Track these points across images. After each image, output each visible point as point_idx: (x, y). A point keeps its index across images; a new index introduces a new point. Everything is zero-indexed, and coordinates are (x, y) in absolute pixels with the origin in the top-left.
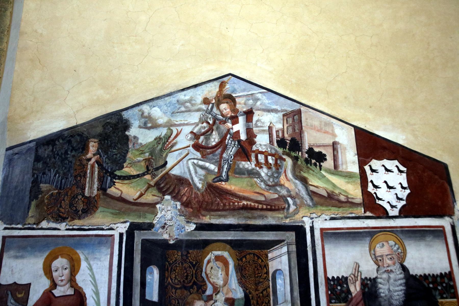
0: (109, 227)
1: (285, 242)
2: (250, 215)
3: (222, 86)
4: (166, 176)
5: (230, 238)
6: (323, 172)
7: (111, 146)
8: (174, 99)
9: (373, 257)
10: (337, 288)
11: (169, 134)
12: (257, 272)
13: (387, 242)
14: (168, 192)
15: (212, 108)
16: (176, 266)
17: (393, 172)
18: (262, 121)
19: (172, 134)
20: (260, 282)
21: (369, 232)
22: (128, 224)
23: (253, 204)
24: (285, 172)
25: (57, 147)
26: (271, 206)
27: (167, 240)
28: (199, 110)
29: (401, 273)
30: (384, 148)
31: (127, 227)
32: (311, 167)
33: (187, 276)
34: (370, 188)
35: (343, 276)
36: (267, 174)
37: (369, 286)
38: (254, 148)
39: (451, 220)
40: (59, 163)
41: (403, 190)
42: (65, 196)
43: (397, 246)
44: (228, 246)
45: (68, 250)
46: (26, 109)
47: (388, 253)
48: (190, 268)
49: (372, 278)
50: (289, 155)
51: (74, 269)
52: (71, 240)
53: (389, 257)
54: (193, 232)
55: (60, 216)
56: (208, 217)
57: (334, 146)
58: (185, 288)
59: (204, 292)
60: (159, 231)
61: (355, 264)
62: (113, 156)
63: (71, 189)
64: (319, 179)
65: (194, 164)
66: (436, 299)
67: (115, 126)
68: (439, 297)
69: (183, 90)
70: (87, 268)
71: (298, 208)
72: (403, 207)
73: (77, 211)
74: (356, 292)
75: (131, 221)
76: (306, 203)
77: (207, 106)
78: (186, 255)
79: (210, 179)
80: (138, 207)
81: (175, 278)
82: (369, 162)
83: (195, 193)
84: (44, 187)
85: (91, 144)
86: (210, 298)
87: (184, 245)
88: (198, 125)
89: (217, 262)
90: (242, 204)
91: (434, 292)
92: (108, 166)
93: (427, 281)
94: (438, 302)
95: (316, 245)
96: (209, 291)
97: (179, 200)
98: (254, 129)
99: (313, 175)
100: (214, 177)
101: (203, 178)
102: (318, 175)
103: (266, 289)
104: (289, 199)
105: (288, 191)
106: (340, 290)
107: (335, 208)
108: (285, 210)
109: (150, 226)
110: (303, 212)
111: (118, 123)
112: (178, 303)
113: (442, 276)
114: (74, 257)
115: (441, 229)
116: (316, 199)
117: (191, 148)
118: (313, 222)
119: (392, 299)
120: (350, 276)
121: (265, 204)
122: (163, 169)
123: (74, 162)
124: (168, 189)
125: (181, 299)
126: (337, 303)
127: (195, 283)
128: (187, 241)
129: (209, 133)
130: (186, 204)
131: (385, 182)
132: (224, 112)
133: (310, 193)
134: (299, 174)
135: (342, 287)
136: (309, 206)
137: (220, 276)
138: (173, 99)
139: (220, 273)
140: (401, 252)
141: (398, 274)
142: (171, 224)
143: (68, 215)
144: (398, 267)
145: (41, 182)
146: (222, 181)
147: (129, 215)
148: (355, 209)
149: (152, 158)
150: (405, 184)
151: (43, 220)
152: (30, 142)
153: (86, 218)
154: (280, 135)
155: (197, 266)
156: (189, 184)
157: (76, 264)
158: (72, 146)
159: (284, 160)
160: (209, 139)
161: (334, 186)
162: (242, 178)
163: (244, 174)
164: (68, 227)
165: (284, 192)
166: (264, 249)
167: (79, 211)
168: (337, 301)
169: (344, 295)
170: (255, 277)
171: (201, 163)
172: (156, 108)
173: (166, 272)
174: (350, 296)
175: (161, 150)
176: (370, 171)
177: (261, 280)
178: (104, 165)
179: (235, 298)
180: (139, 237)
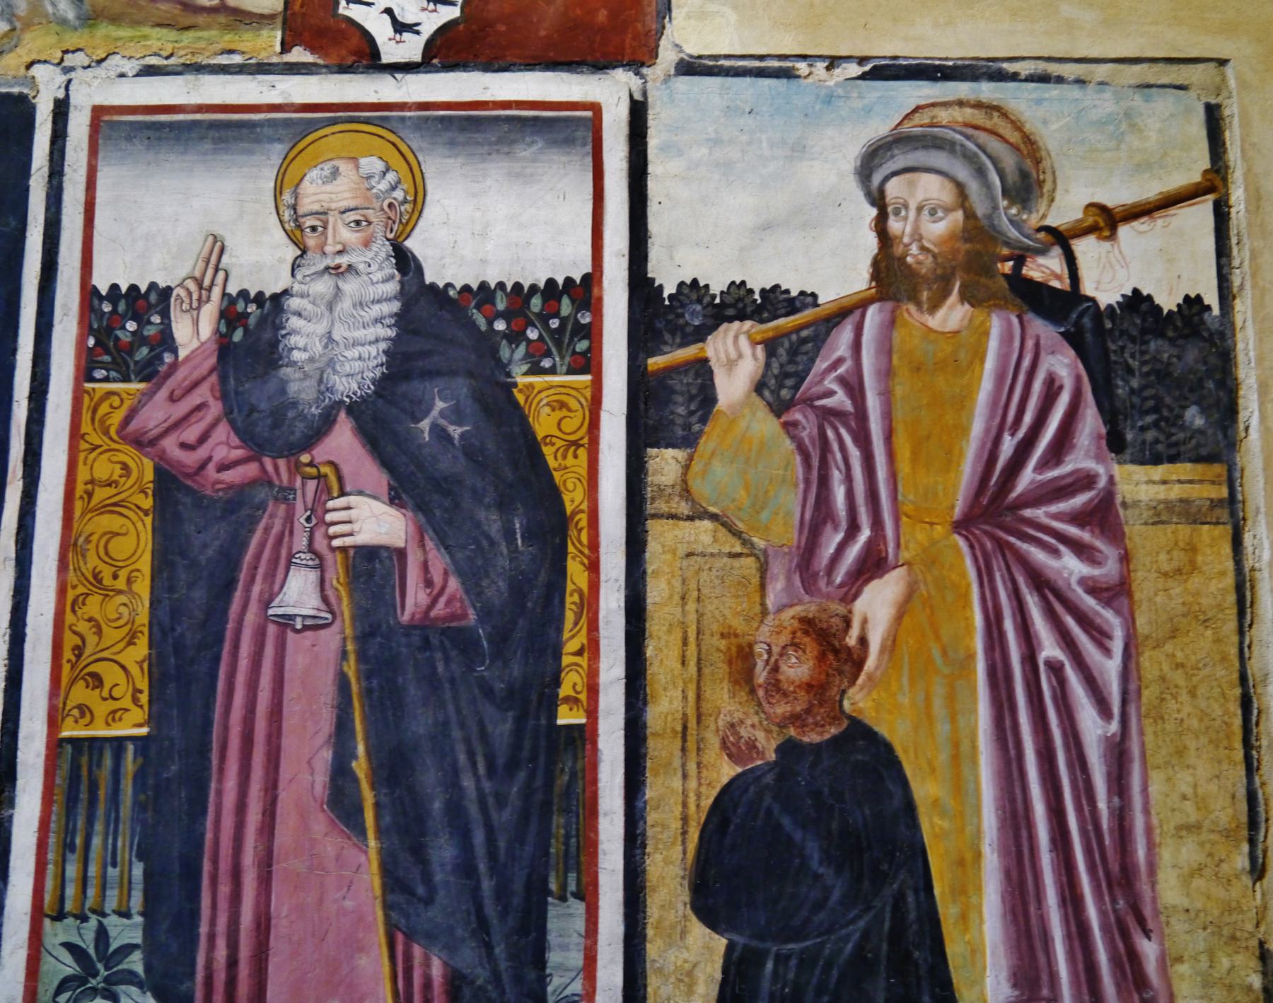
9: (287, 215)
10: (123, 328)
13: (354, 159)
21: (287, 123)
35: (153, 286)
37: (252, 321)
43: (391, 177)
47: (352, 204)
49: (268, 294)
53: (352, 216)
61: (211, 239)
66: (509, 375)
68: (525, 368)
74: (195, 344)
76: (50, 9)
91: (505, 353)
93: (488, 306)
94: (515, 385)
95: (66, 169)
106: (133, 333)
107: (165, 31)
113: (551, 289)
115: (589, 114)
118: (70, 81)
119: (335, 372)
126: (115, 381)
136: (63, 22)
140: (405, 201)
141: (377, 284)
144: (383, 255)
148: (248, 36)
168: (113, 374)
169: (145, 351)
174: (168, 358)
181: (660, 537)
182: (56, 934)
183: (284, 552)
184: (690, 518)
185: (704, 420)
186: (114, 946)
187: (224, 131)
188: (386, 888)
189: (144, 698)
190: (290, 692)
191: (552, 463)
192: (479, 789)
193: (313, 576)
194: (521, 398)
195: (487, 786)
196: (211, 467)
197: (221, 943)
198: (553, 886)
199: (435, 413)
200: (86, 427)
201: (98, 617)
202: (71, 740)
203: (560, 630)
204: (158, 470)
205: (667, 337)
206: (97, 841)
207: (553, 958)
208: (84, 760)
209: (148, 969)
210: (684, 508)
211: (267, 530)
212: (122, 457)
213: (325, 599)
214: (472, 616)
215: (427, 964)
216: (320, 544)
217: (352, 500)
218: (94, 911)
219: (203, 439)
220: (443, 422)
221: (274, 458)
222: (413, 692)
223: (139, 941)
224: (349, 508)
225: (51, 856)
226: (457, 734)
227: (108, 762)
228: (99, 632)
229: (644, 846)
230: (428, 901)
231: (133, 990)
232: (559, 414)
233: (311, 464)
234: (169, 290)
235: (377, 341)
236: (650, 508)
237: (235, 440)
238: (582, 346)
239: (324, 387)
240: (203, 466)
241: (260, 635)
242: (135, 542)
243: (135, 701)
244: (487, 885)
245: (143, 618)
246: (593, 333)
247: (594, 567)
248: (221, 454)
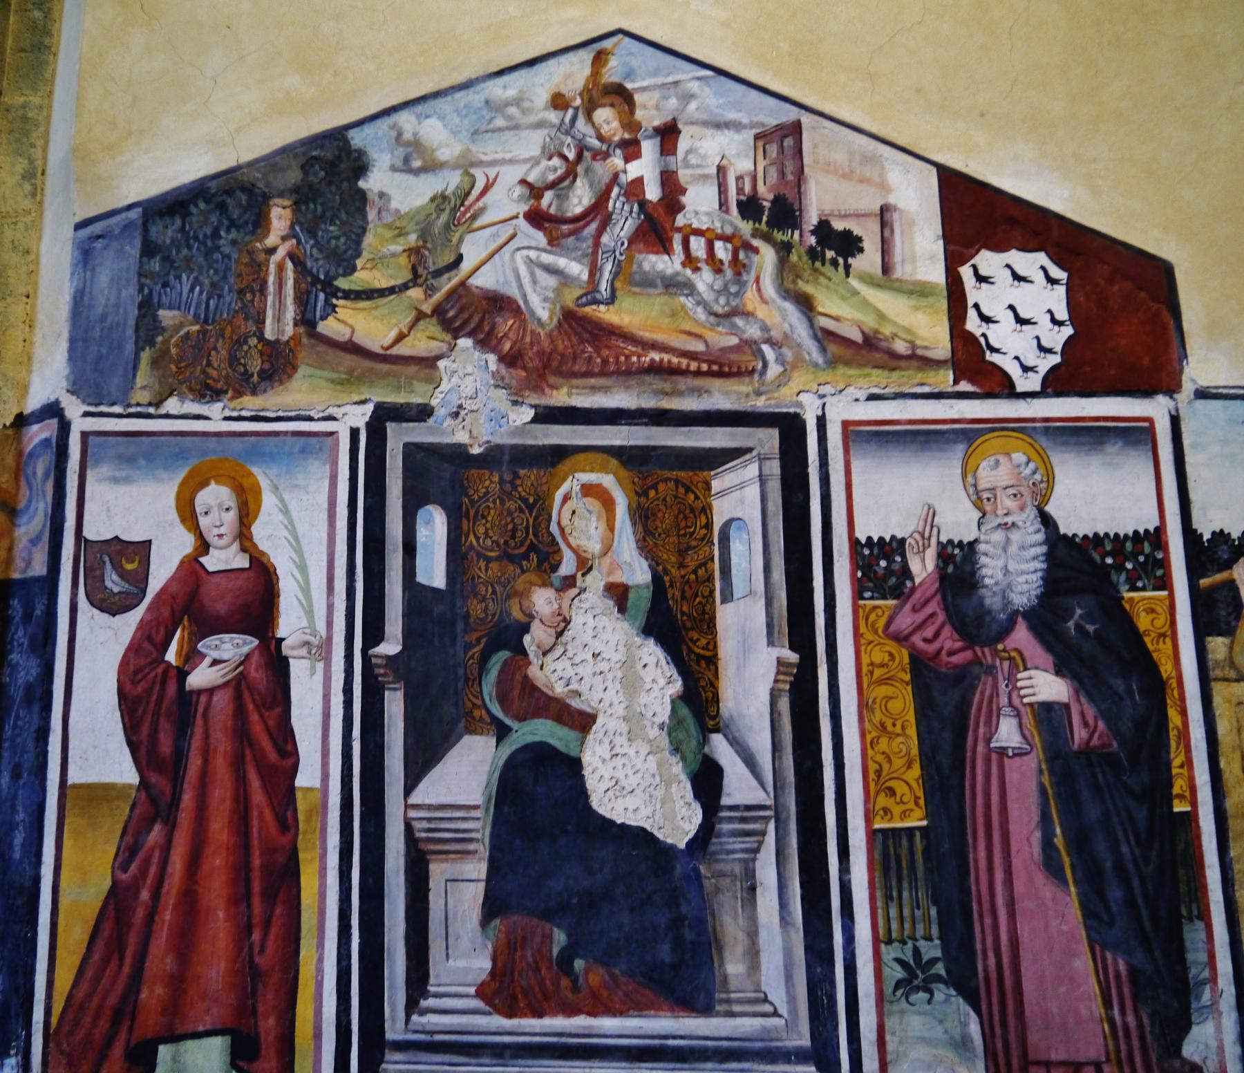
0: (326, 414)
1: (755, 453)
2: (667, 386)
3: (600, 59)
4: (461, 291)
5: (617, 443)
6: (853, 282)
7: (323, 216)
8: (477, 97)
9: (971, 490)
10: (878, 564)
11: (467, 188)
12: (683, 524)
13: (1008, 454)
14: (467, 330)
15: (574, 120)
16: (488, 507)
17: (1031, 282)
18: (702, 151)
19: (472, 187)
20: (689, 548)
21: (963, 431)
22: (369, 408)
23: (675, 360)
24: (757, 281)
25: (194, 219)
26: (721, 365)
27: (465, 445)
28: (540, 125)
29: (1038, 531)
30: (1013, 222)
31: (369, 414)
32: (823, 269)
33: (514, 530)
34: (973, 324)
35: (893, 537)
36: (711, 287)
37: (958, 559)
38: (680, 220)
39: (1171, 404)
40: (201, 259)
41: (1056, 328)
42: (217, 341)
43: (1032, 465)
44: (614, 462)
45: (228, 467)
46: (114, 125)
47: (1010, 483)
48: (521, 511)
50: (767, 238)
51: (247, 512)
52: (236, 444)
53: (1011, 491)
54: (528, 426)
55: (208, 387)
56: (565, 390)
57: (885, 215)
58: (511, 558)
59: (555, 568)
60: (445, 424)
62: (329, 242)
63: (230, 322)
64: (844, 299)
65: (530, 262)
66: (1118, 592)
67: (332, 167)
68: (1127, 587)
69: (500, 73)
70: (277, 510)
71: (789, 369)
72: (1054, 369)
73: (247, 376)
74: (924, 575)
75: (376, 399)
77: (561, 113)
78: (512, 482)
79: (570, 297)
80: (395, 368)
81: (486, 535)
82: (972, 257)
83: (533, 332)
84: (167, 316)
85: (275, 212)
86: (569, 582)
87: (506, 457)
88: (538, 163)
89: (585, 500)
90: (648, 359)
91: (1114, 577)
92: (320, 267)
94: (1123, 598)
96: (567, 566)
97: (493, 350)
98: (681, 173)
99: (828, 288)
100: (579, 292)
101: (551, 295)
102: (840, 289)
103: (704, 564)
104: (766, 348)
105: (765, 328)
106: (885, 568)
107: (879, 372)
108: (756, 377)
109: (423, 413)
110: (799, 380)
111: (339, 158)
112: (494, 592)
114: (246, 483)
115: (1146, 424)
116: (833, 348)
117: (522, 222)
118: (824, 404)
120: (911, 536)
121: (704, 361)
122: (453, 273)
123: (235, 256)
124: (466, 323)
125: (499, 583)
126: (877, 599)
127: (532, 548)
128: (514, 447)
129: (567, 183)
130: (511, 360)
131: (1011, 307)
132: (605, 130)
133: (819, 334)
134: (791, 286)
135: (890, 561)
136: (816, 365)
137: (592, 531)
138: (474, 97)
139: (594, 525)
140: (1042, 481)
142: (475, 408)
143: (227, 383)
144: (1032, 516)
145: (160, 306)
146: (598, 302)
147: (371, 384)
148: (932, 374)
149: (424, 247)
150: (1062, 314)
151: (171, 395)
152: (130, 207)
153: (270, 392)
154: (747, 188)
155: (539, 506)
156: (517, 311)
157: (250, 499)
158: (228, 218)
159: (756, 251)
160: (567, 197)
161: (882, 317)
162: (649, 295)
163: (655, 286)
164: (227, 413)
165: (753, 332)
166: (702, 469)
167: (252, 375)
168: (876, 595)
169: (894, 579)
170: (678, 535)
171: (547, 258)
172: (433, 121)
173: (465, 522)
174: (909, 584)
175: (447, 227)
176: (974, 280)
177: (693, 543)
178: (309, 264)
179: (630, 583)
180: (397, 437)
181: (1220, 692)
182: (889, 953)
183: (994, 707)
184: (1237, 681)
185: (1238, 618)
186: (925, 958)
187: (923, 438)
188: (1083, 916)
189: (922, 802)
190: (1011, 794)
191: (1150, 647)
192: (1132, 853)
193: (1014, 722)
194: (1127, 606)
195: (1137, 851)
196: (944, 653)
197: (991, 955)
198: (1184, 912)
199: (1076, 616)
200: (863, 629)
201: (887, 751)
202: (883, 831)
203: (1168, 752)
204: (911, 656)
205: (1209, 566)
206: (905, 894)
207: (1190, 956)
208: (891, 842)
209: (948, 971)
210: (1233, 674)
211: (983, 693)
212: (888, 648)
213: (1024, 736)
214: (1115, 745)
215: (1116, 963)
216: (1016, 701)
217: (1032, 672)
218: (910, 938)
219: (937, 635)
220: (1082, 622)
221: (982, 647)
222: (1086, 794)
223: (938, 953)
224: (1030, 678)
225: (879, 904)
226: (1115, 819)
227: (905, 843)
228: (890, 761)
229: (1233, 885)
230: (1111, 924)
231: (941, 986)
232: (1151, 616)
233: (1004, 650)
234: (903, 541)
235: (1036, 571)
236: (1212, 674)
237: (956, 636)
238: (1159, 573)
239: (1007, 602)
240: (939, 652)
241: (988, 760)
242: (903, 702)
243: (917, 804)
244: (1144, 913)
245: (915, 751)
246: (1165, 564)
247: (1184, 712)
248: (948, 645)
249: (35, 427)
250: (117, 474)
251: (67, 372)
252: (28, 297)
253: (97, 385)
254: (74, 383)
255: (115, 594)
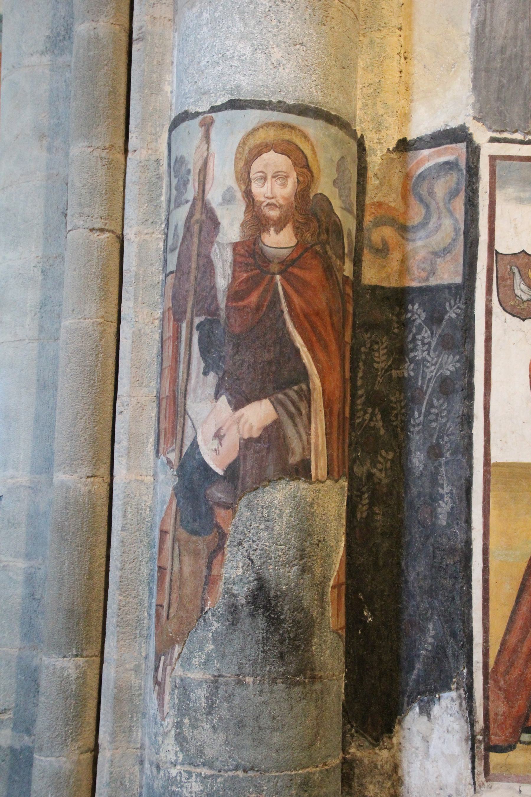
249: (426, 152)
250: (522, 195)
251: (472, 100)
252: (400, 29)
253: (500, 113)
254: (480, 111)
255: (524, 301)
